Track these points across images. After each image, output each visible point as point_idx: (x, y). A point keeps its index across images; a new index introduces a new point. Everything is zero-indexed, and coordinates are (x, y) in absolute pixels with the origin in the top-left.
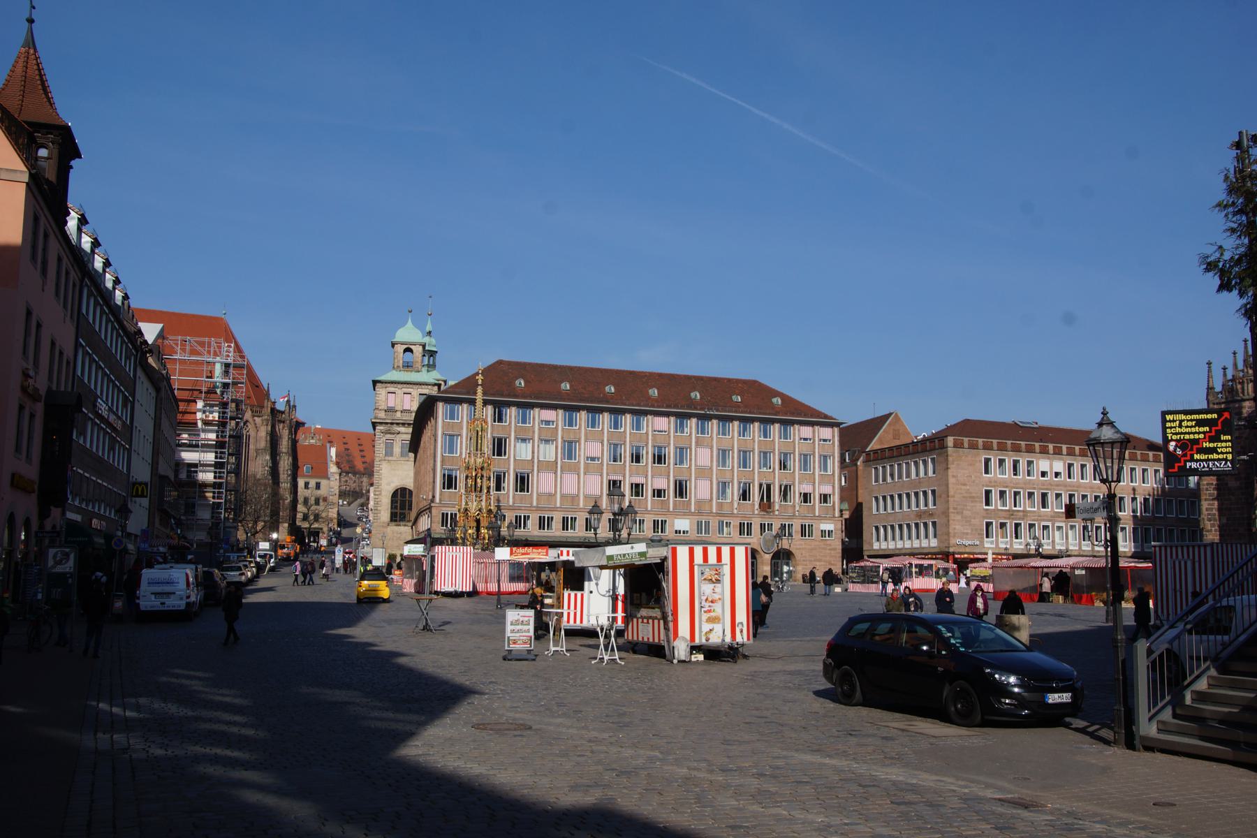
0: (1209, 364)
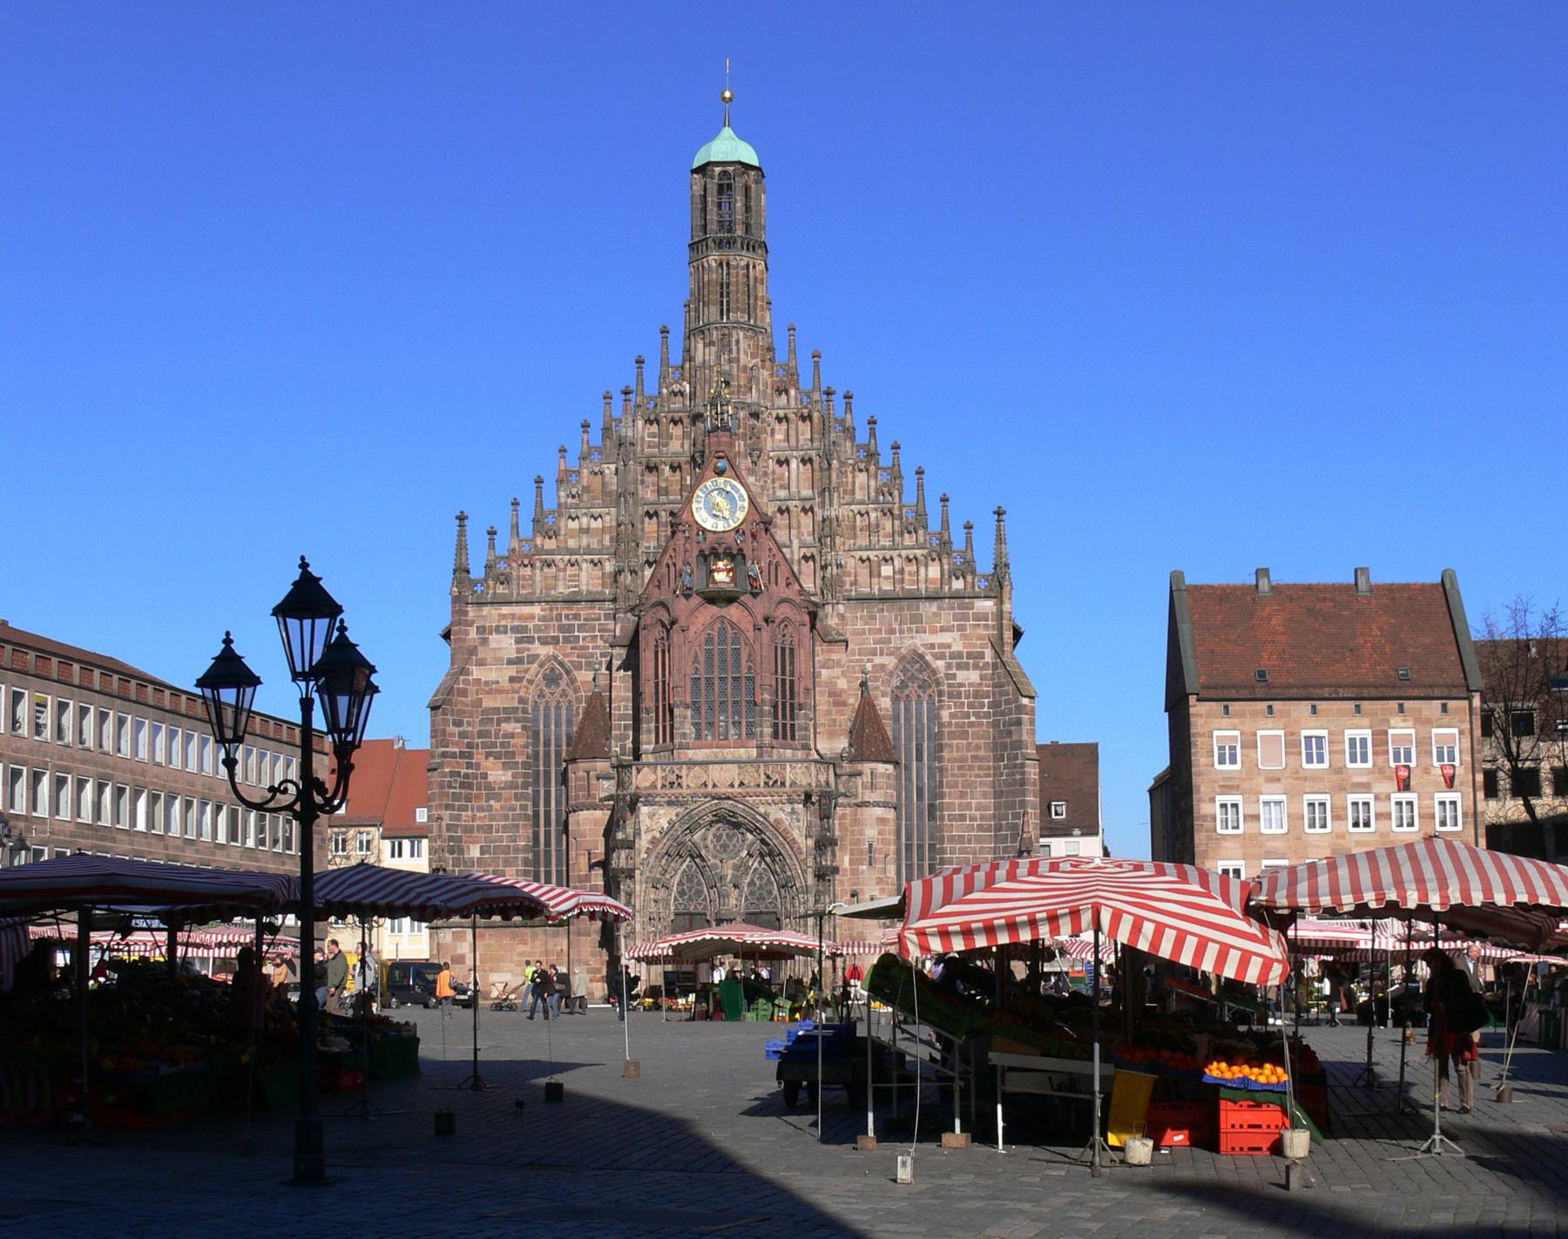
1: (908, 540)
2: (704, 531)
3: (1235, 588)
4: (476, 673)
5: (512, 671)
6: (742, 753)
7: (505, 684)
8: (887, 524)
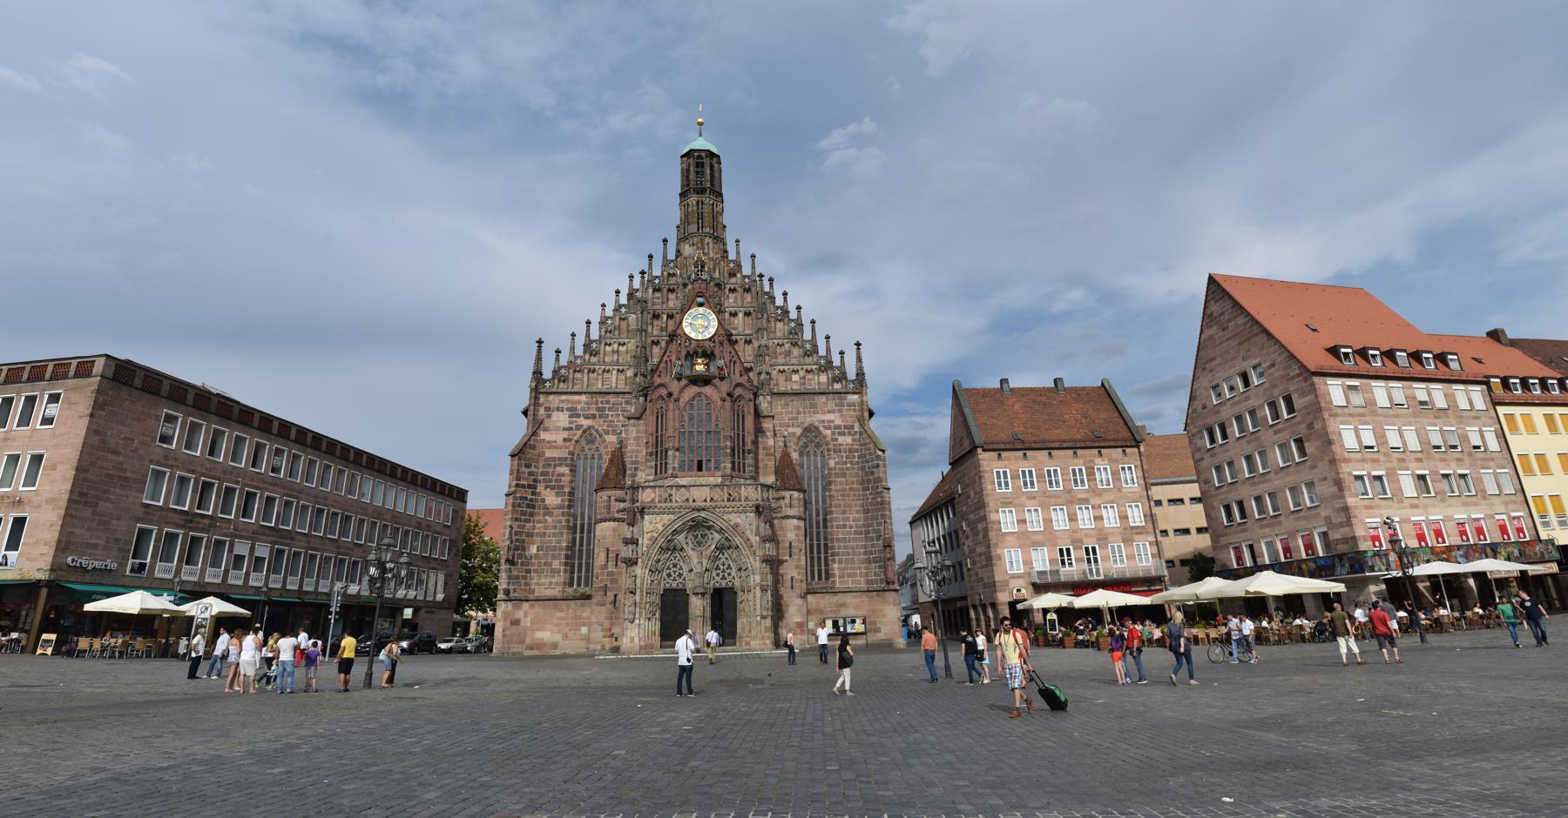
0: (540, 342)
1: (808, 360)
2: (690, 339)
3: (989, 390)
4: (543, 435)
5: (566, 435)
6: (712, 480)
7: (560, 442)
8: (796, 351)
